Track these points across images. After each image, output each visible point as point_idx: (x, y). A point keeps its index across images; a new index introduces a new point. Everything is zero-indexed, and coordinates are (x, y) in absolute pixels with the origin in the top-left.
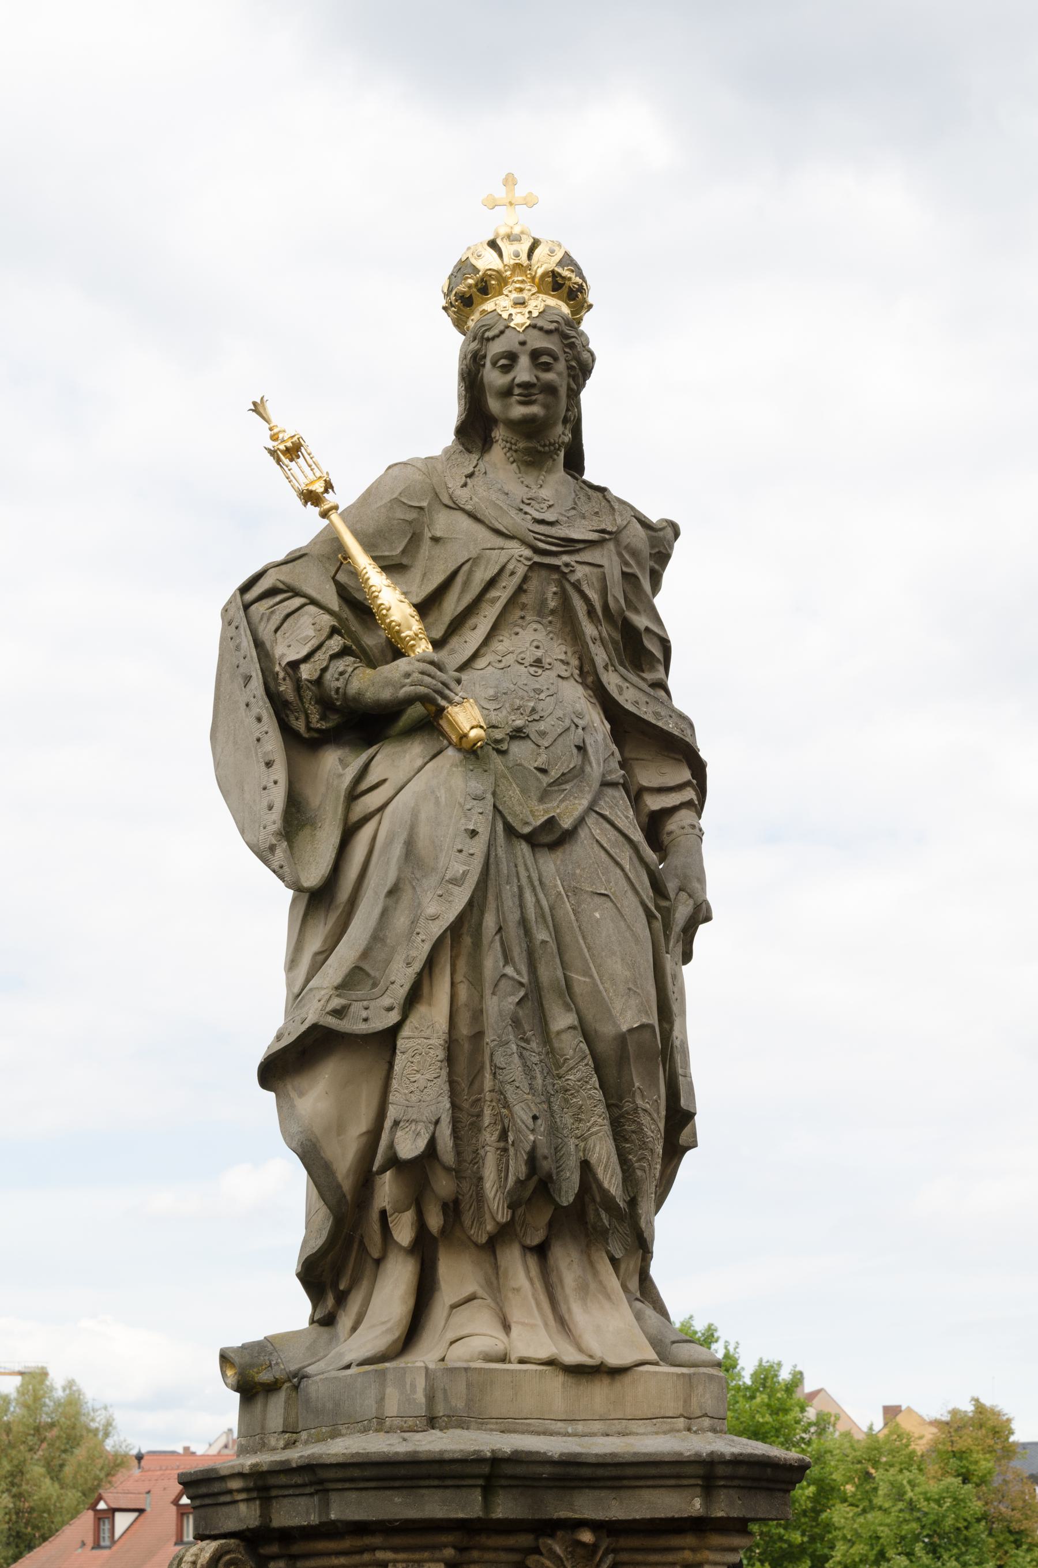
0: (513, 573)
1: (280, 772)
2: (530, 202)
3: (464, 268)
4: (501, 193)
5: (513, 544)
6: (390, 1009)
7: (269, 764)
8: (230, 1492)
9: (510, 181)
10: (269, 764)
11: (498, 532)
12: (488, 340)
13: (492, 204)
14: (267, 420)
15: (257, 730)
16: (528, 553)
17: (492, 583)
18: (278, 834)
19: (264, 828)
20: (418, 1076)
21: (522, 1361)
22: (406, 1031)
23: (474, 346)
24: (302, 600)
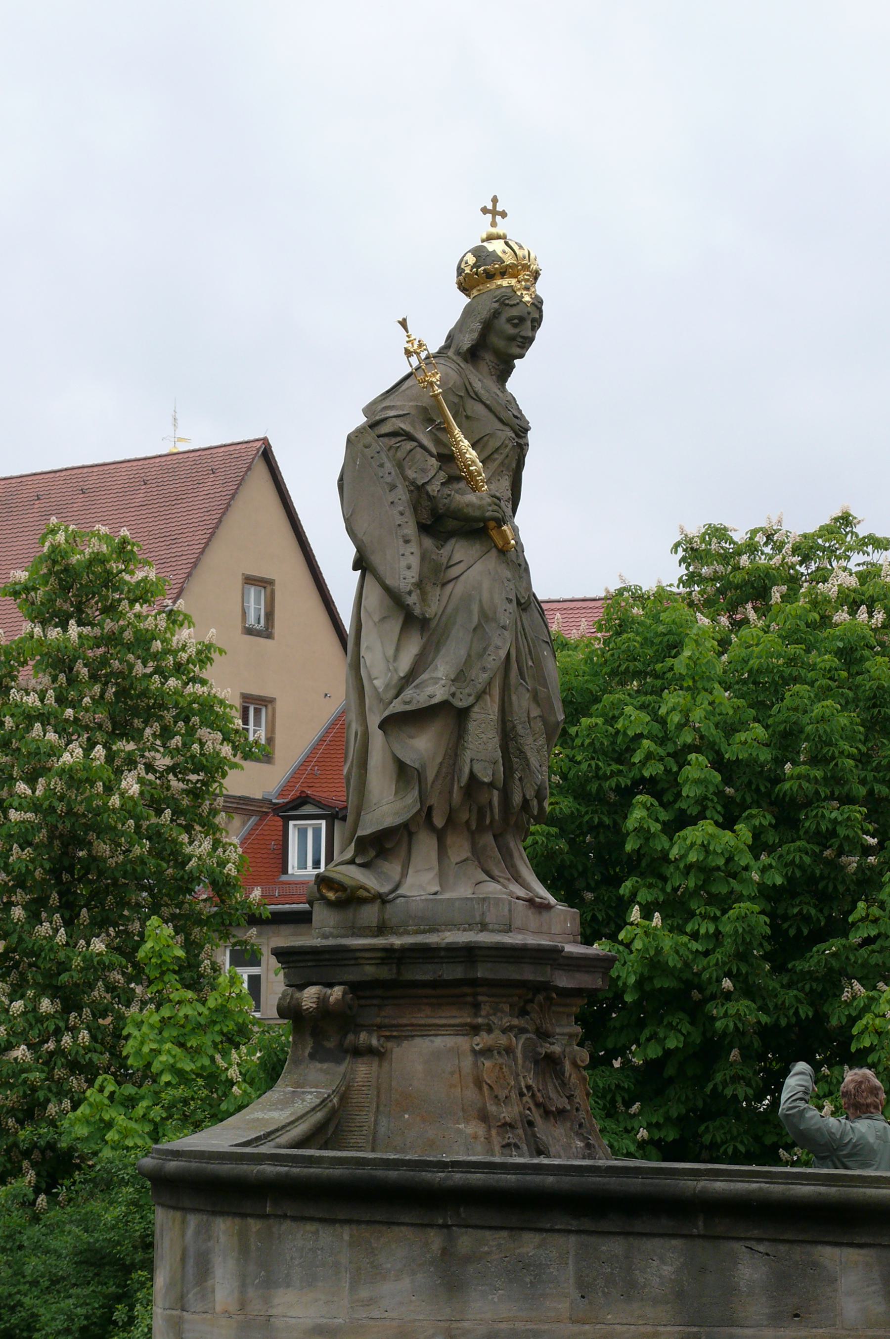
0: (507, 446)
1: (413, 547)
2: (504, 214)
3: (478, 252)
4: (490, 206)
5: (507, 429)
6: (470, 695)
7: (407, 542)
8: (356, 959)
9: (495, 200)
10: (407, 542)
11: (501, 420)
12: (507, 305)
13: (485, 211)
14: (407, 331)
15: (399, 520)
16: (513, 435)
17: (497, 450)
18: (414, 584)
19: (404, 579)
20: (483, 735)
21: (518, 898)
22: (476, 709)
23: (496, 305)
24: (415, 444)
